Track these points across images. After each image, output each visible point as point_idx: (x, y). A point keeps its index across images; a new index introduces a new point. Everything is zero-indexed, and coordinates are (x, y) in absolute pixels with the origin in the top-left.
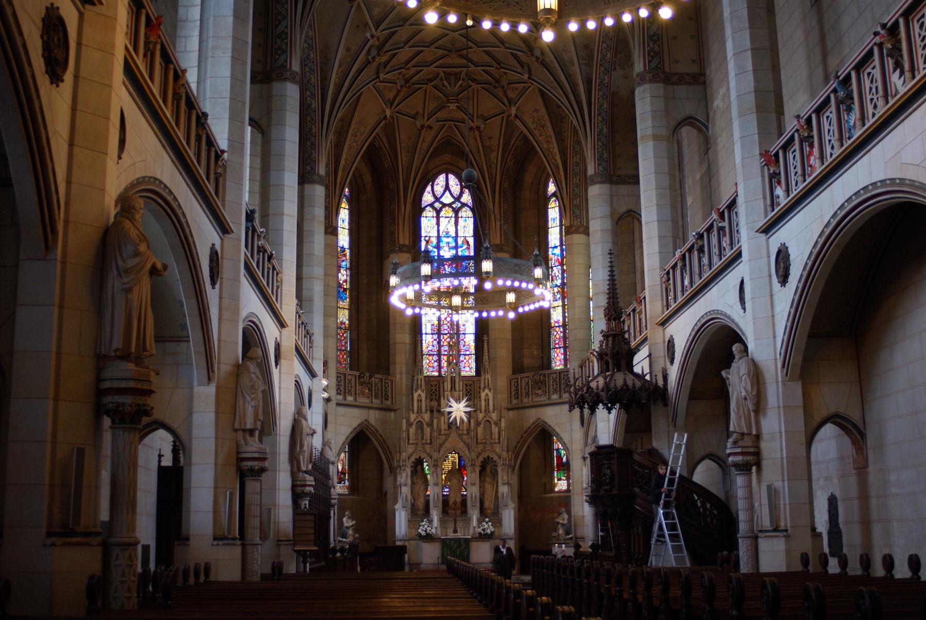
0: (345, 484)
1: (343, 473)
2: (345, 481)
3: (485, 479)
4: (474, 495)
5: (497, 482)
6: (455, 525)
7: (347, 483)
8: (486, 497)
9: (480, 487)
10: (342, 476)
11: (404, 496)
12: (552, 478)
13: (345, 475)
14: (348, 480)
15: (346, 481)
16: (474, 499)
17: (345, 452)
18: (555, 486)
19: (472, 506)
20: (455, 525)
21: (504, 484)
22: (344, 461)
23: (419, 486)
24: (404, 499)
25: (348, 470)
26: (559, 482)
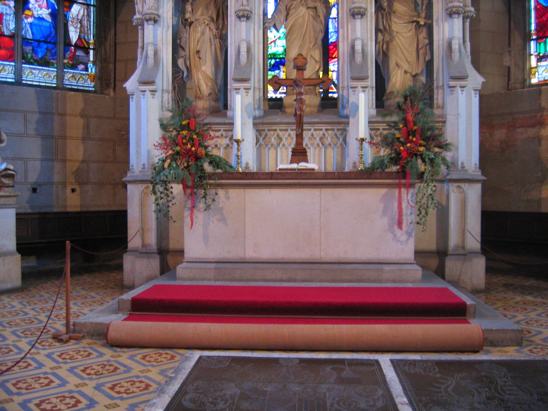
0: (86, 69)
1: (82, 46)
2: (86, 65)
3: (390, 5)
4: (358, 47)
5: (429, 16)
6: (300, 137)
7: (92, 70)
8: (392, 61)
9: (377, 30)
10: (79, 53)
11: (151, 53)
12: (525, 55)
13: (88, 53)
14: (94, 63)
15: (90, 65)
16: (359, 58)
17: (88, 5)
18: (530, 72)
19: (354, 79)
20: (300, 137)
21: (451, 14)
22: (85, 23)
23: (200, 29)
24: (151, 61)
25: (95, 44)
26: (543, 63)
